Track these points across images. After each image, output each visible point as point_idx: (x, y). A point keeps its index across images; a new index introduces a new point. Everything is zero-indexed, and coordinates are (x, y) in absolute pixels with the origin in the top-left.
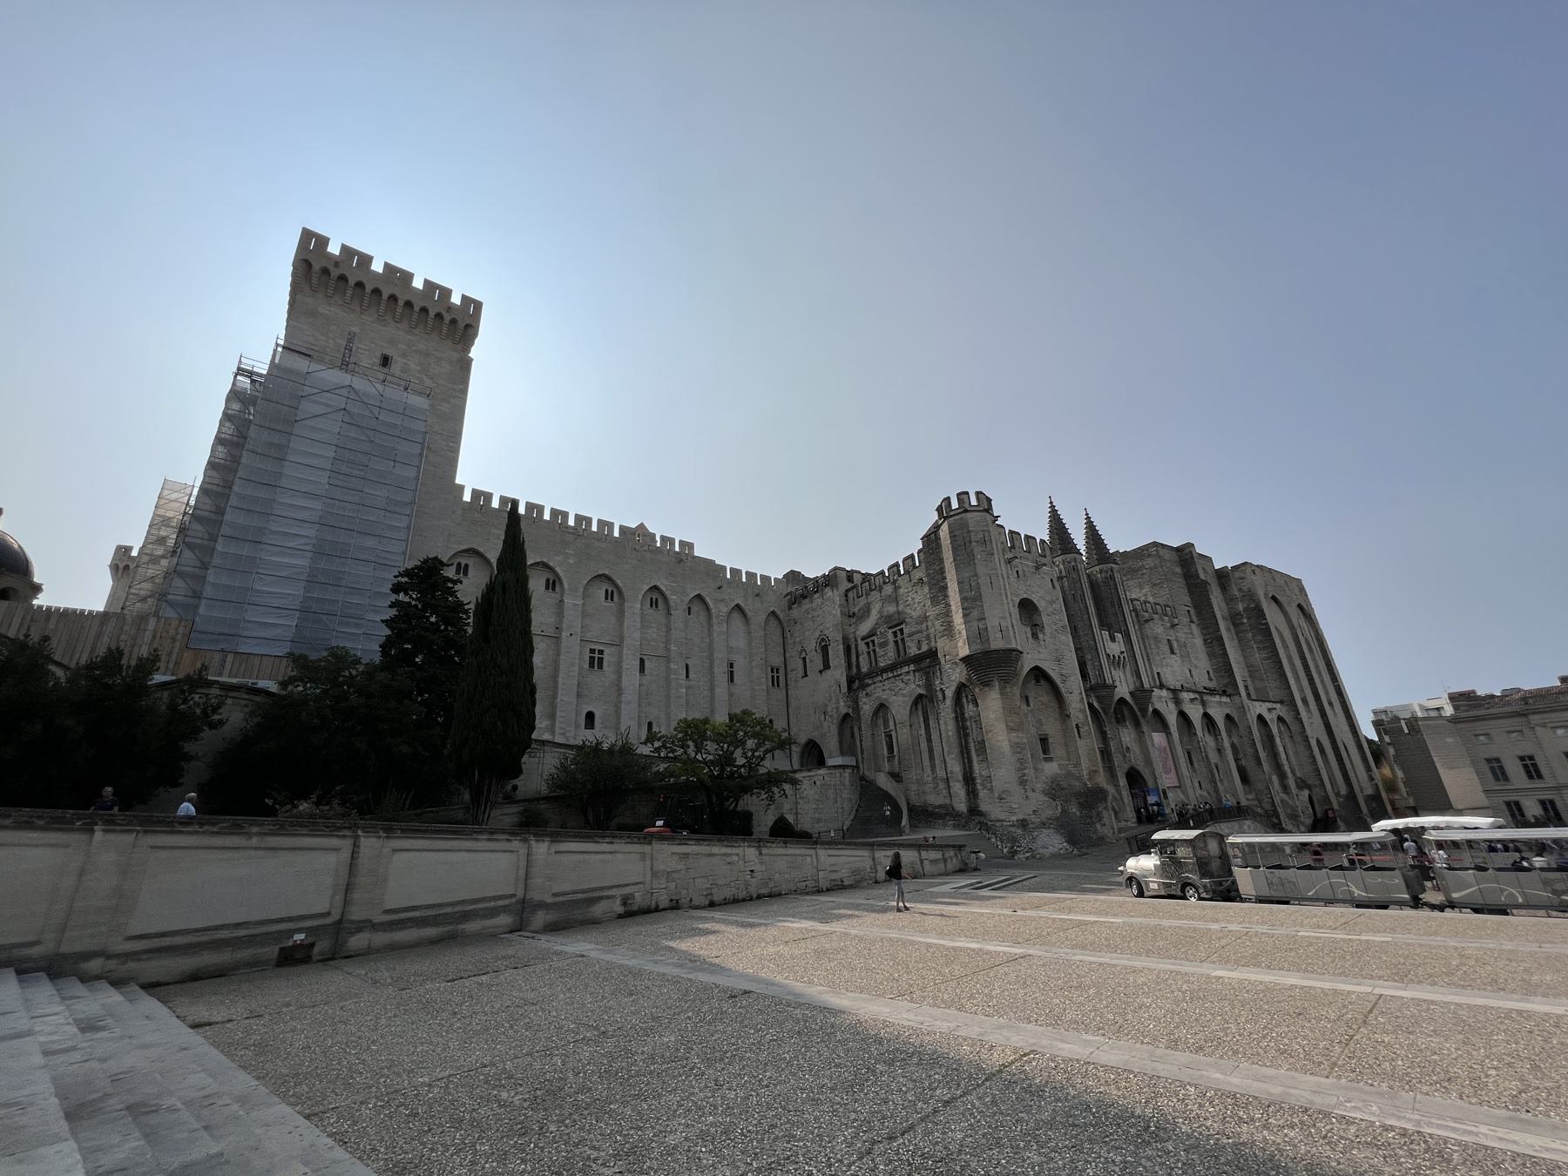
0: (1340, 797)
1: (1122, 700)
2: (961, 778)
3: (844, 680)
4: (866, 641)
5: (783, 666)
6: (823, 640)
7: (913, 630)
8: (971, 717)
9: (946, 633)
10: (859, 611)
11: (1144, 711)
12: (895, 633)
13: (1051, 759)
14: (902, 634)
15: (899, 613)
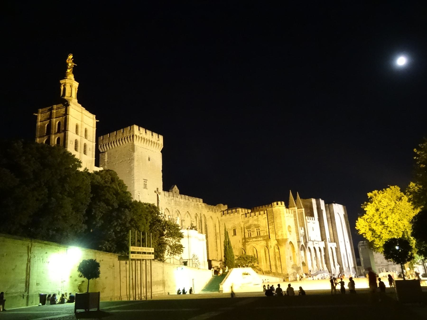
0: (346, 267)
1: (302, 245)
2: (274, 265)
3: (241, 239)
4: (248, 230)
5: (219, 233)
6: (234, 227)
7: (262, 229)
8: (277, 252)
9: (272, 233)
10: (245, 221)
11: (306, 247)
12: (257, 230)
13: (292, 261)
14: (259, 230)
15: (258, 224)
